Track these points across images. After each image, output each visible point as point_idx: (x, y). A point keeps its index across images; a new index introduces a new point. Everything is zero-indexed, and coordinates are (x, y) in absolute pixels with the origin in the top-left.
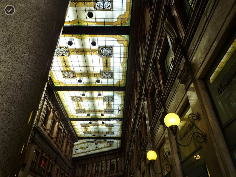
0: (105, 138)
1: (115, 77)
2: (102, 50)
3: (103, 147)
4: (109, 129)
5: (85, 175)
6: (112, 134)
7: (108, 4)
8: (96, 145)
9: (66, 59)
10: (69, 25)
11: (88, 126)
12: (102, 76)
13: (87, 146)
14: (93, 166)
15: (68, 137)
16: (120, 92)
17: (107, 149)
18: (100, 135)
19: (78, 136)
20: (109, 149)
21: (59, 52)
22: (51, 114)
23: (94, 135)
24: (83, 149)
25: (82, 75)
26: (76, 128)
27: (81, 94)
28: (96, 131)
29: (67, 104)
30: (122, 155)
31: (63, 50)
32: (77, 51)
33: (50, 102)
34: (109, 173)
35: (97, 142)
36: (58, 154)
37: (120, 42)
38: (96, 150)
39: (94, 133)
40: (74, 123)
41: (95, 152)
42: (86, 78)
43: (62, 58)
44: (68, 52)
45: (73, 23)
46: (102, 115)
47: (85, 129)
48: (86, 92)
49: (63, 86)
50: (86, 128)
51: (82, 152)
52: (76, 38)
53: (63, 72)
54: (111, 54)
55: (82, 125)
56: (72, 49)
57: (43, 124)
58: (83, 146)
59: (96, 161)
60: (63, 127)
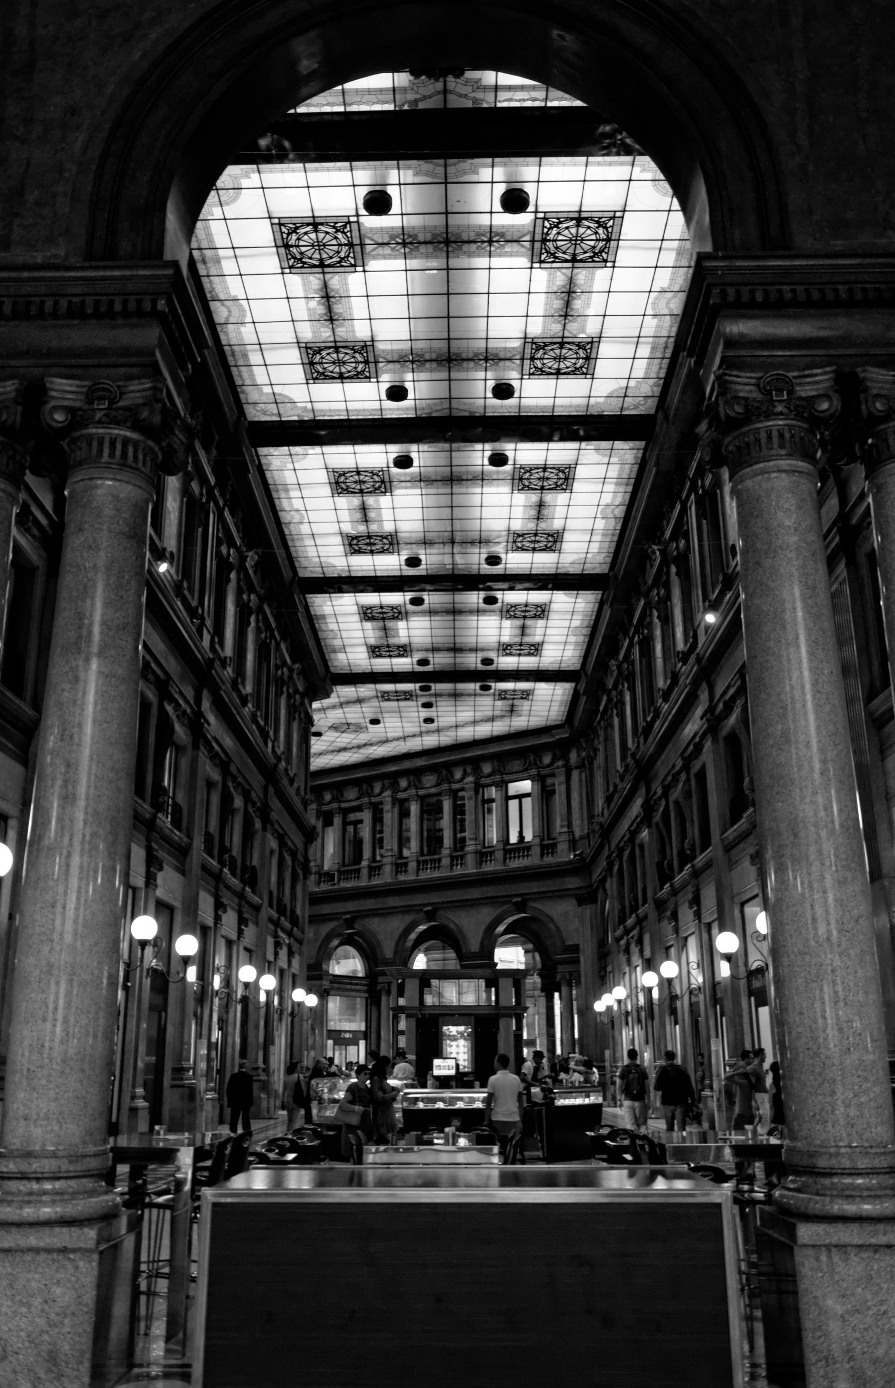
0: (487, 676)
2: (555, 231)
3: (469, 718)
4: (519, 632)
5: (365, 863)
6: (529, 654)
8: (425, 713)
9: (335, 281)
10: (390, 107)
12: (527, 362)
13: (373, 716)
14: (404, 814)
15: (290, 677)
17: (484, 731)
18: (458, 660)
19: (333, 670)
20: (499, 728)
21: (303, 249)
22: (233, 575)
23: (423, 662)
24: (351, 732)
25: (413, 359)
26: (333, 626)
29: (302, 507)
30: (573, 757)
31: (328, 237)
32: (406, 242)
33: (227, 513)
34: (499, 855)
35: (436, 695)
36: (270, 774)
38: (421, 734)
39: (427, 650)
41: (415, 745)
43: (315, 280)
47: (381, 633)
48: (424, 447)
49: (296, 418)
50: (385, 629)
51: (343, 745)
55: (367, 614)
56: (382, 228)
57: (216, 640)
58: (353, 714)
59: (421, 792)
60: (273, 636)
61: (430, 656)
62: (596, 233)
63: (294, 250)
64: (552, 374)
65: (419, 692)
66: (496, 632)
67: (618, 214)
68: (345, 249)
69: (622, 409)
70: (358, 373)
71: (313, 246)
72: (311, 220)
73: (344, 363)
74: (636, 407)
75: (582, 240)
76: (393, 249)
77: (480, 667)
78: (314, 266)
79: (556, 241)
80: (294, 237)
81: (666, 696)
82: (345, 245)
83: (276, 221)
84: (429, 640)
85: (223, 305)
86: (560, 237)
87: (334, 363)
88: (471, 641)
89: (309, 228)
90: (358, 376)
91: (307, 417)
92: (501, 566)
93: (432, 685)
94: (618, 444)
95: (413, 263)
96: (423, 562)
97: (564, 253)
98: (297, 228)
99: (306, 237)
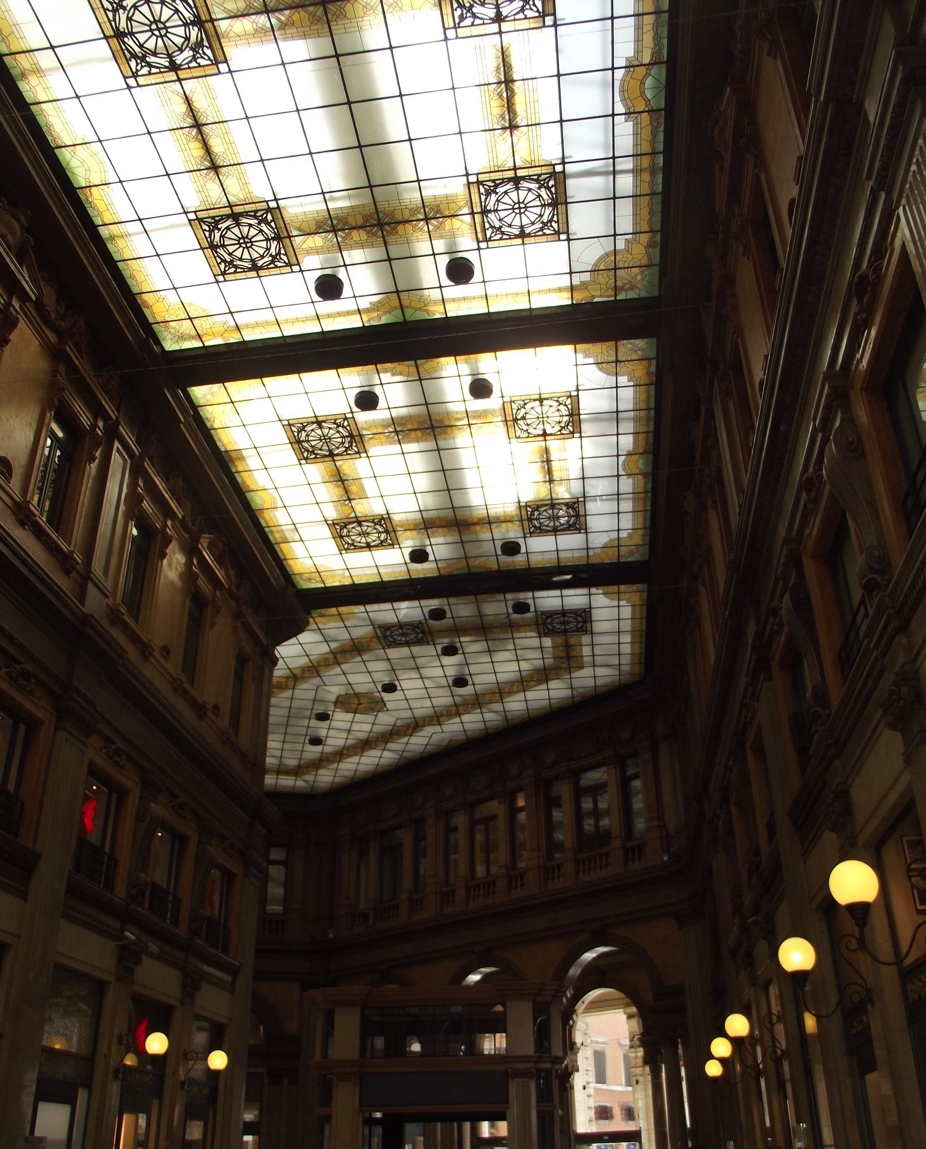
7: (541, 216)
21: (313, 443)
27: (426, 610)
31: (332, 432)
37: (614, 365)
42: (449, 539)
45: (375, 314)
48: (452, 600)
49: (337, 584)
52: (393, 375)
53: (334, 524)
63: (305, 445)
64: (549, 531)
70: (382, 542)
71: (321, 440)
72: (314, 419)
73: (368, 534)
74: (631, 553)
78: (326, 456)
80: (304, 434)
83: (286, 423)
87: (360, 535)
89: (315, 426)
90: (381, 545)
91: (348, 582)
94: (623, 588)
95: (407, 447)
98: (304, 427)
99: (313, 434)
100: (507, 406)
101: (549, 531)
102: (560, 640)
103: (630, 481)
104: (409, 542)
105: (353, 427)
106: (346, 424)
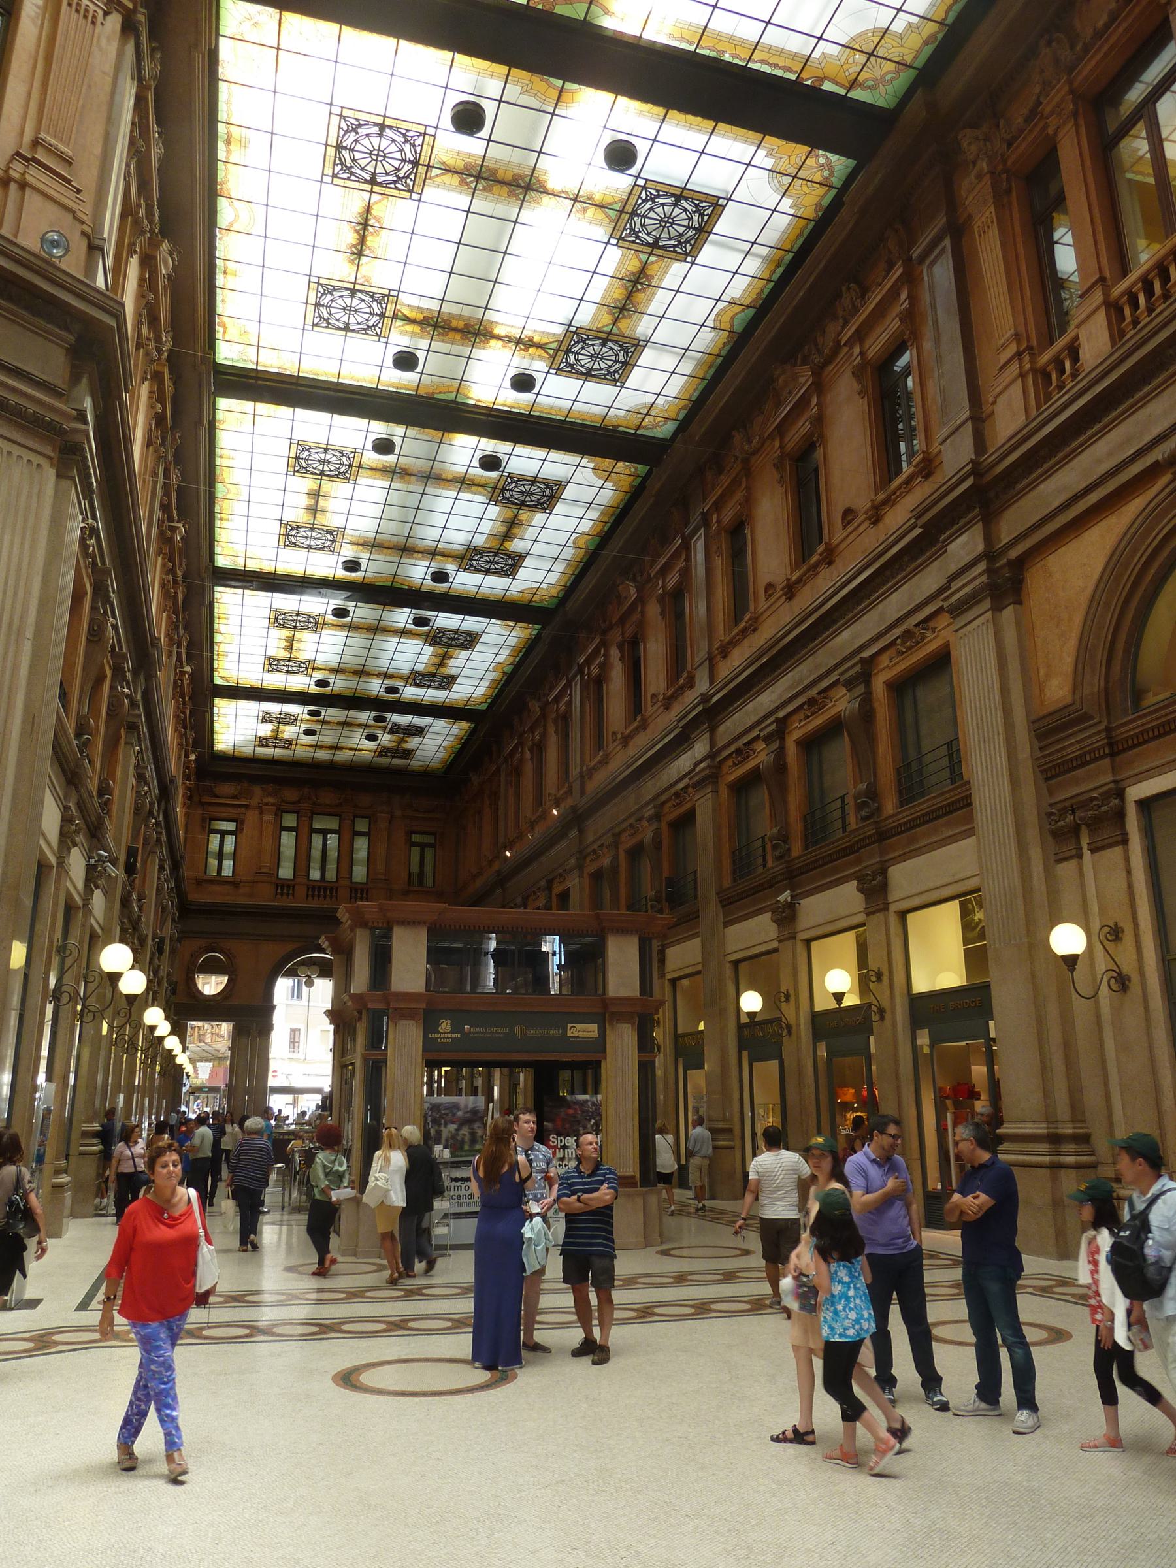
1: (636, 377)
4: (436, 660)
6: (439, 687)
11: (315, 624)
16: (620, 464)
23: (321, 683)
25: (436, 324)
27: (372, 437)
28: (353, 660)
31: (393, 148)
35: (324, 722)
39: (331, 670)
40: (227, 599)
44: (422, 169)
46: (440, 577)
48: (412, 431)
54: (689, 244)
55: (278, 620)
61: (331, 677)
62: (690, 219)
63: (345, 154)
65: (306, 717)
66: (413, 657)
67: (721, 202)
68: (408, 167)
69: (639, 427)
73: (356, 311)
75: (672, 224)
76: (463, 182)
77: (383, 693)
79: (644, 217)
81: (626, 740)
82: (410, 162)
84: (337, 658)
85: (231, 204)
86: (652, 214)
88: (382, 665)
91: (291, 370)
92: (447, 585)
93: (323, 710)
95: (479, 205)
96: (363, 568)
97: (648, 234)
98: (360, 126)
99: (366, 142)
100: (637, 190)
101: (582, 373)
102: (508, 513)
103: (712, 334)
104: (401, 338)
105: (426, 151)
106: (419, 141)
